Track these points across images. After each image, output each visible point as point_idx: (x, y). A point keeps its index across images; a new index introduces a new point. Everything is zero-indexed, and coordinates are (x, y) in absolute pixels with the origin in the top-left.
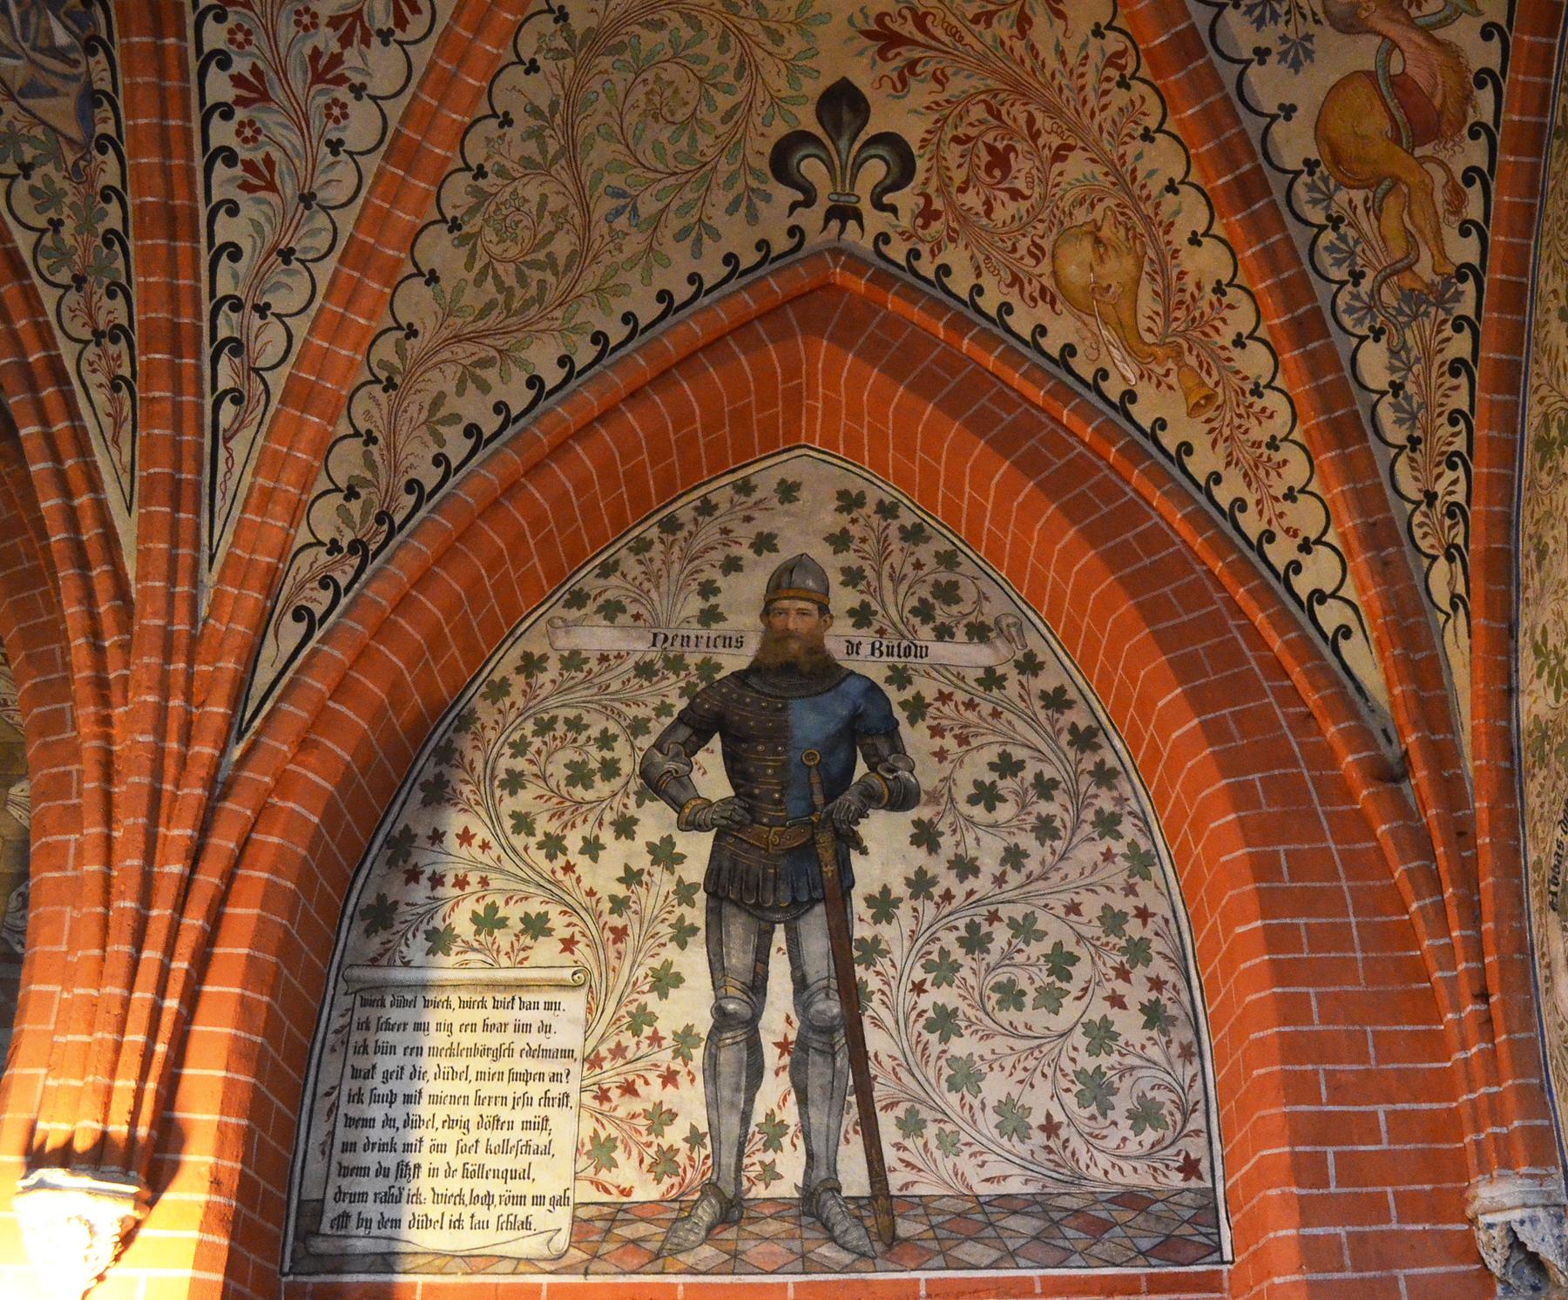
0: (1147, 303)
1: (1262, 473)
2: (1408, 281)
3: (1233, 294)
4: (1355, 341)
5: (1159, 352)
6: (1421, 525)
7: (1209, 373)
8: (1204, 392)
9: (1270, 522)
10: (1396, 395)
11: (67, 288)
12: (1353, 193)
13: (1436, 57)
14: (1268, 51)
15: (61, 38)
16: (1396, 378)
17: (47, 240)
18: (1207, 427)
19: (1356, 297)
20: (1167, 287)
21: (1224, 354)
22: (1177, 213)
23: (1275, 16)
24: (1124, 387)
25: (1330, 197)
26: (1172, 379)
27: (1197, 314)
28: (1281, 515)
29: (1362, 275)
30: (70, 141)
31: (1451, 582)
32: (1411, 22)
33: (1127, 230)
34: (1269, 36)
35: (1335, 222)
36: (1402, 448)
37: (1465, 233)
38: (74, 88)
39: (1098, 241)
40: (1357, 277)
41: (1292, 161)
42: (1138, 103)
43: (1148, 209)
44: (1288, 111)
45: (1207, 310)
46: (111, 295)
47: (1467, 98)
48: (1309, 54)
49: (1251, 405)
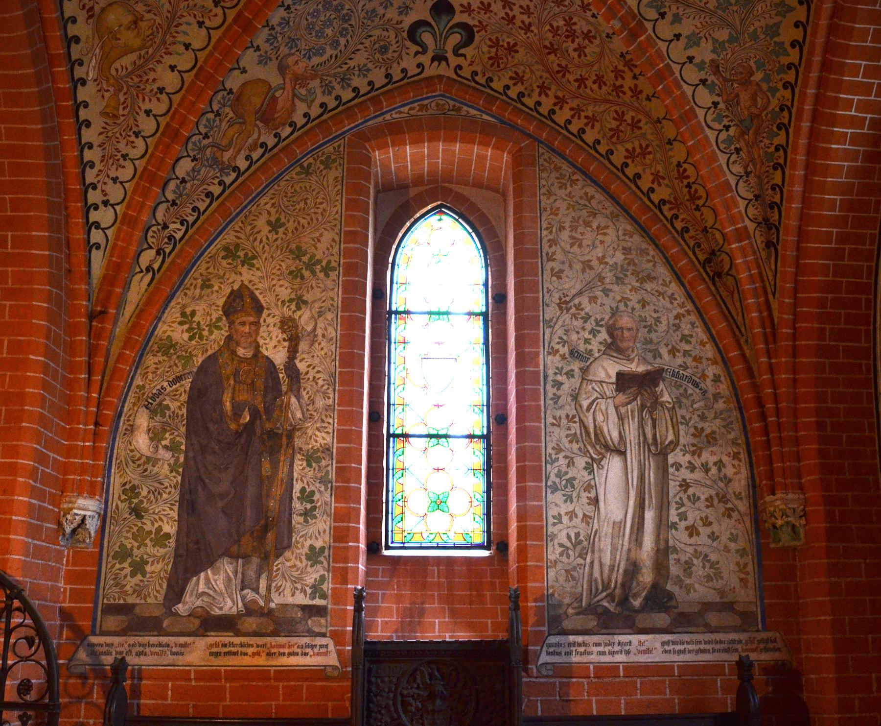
0: (128, 61)
1: (111, 161)
2: (218, 154)
3: (164, 97)
4: (186, 154)
5: (112, 81)
6: (154, 232)
7: (124, 109)
8: (116, 113)
9: (99, 182)
10: (181, 183)
12: (231, 112)
13: (289, 103)
14: (260, 50)
16: (187, 178)
18: (104, 125)
19: (200, 141)
20: (142, 66)
21: (137, 109)
22: (178, 54)
23: (272, 44)
24: (84, 76)
25: (224, 106)
26: (107, 95)
27: (142, 87)
28: (105, 183)
29: (208, 138)
31: (153, 261)
32: (294, 88)
33: (152, 34)
34: (265, 47)
35: (218, 114)
36: (168, 201)
37: (247, 159)
39: (135, 23)
40: (206, 136)
41: (228, 85)
42: (212, 14)
43: (169, 39)
44: (244, 71)
45: (148, 90)
47: (284, 124)
48: (266, 63)
49: (130, 136)
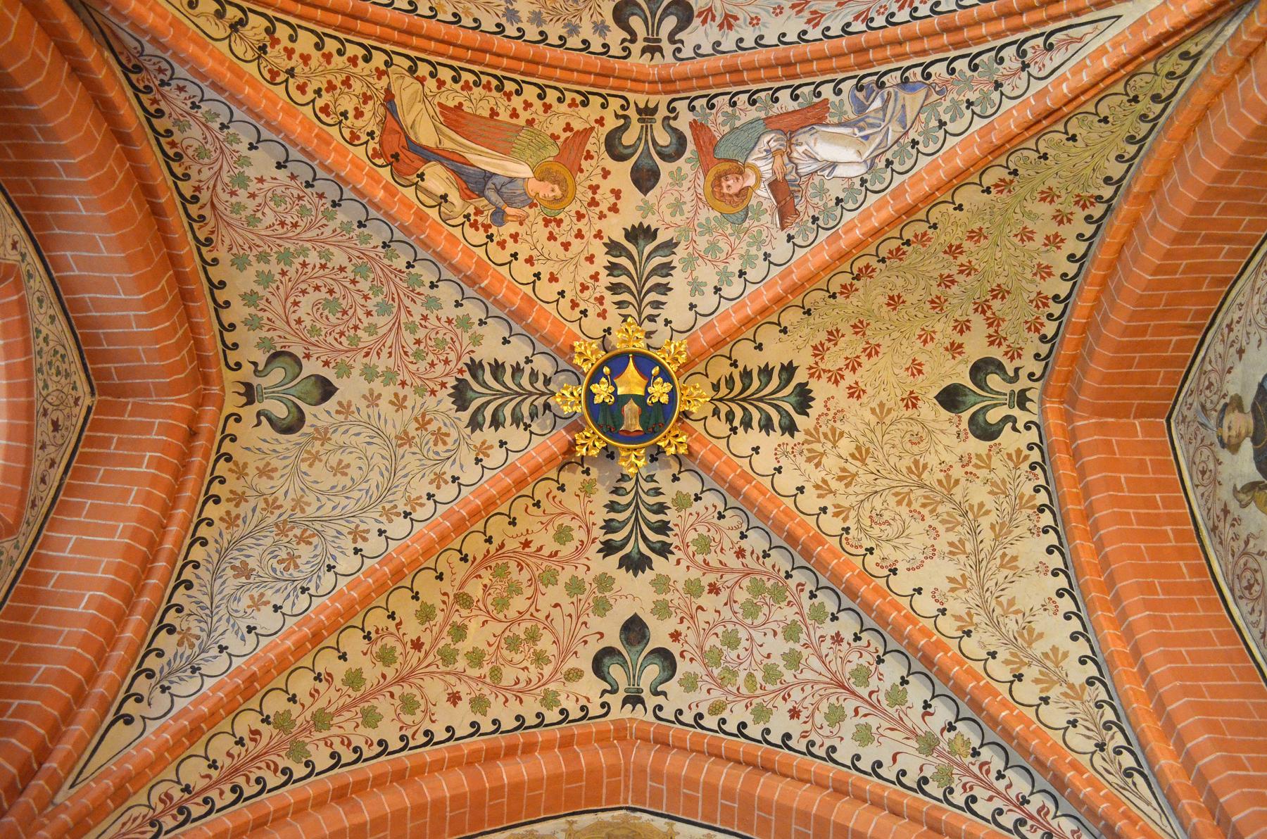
11: (1002, 94)
15: (878, 104)
17: (977, 109)
30: (927, 97)
38: (901, 94)
46: (1002, 60)
